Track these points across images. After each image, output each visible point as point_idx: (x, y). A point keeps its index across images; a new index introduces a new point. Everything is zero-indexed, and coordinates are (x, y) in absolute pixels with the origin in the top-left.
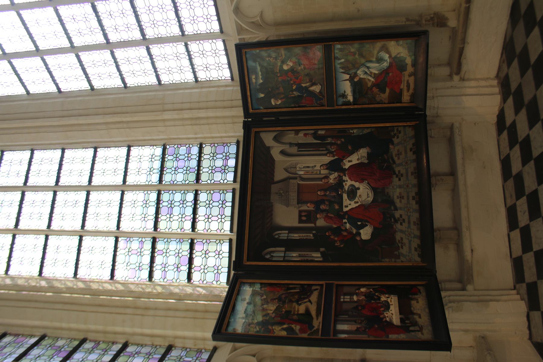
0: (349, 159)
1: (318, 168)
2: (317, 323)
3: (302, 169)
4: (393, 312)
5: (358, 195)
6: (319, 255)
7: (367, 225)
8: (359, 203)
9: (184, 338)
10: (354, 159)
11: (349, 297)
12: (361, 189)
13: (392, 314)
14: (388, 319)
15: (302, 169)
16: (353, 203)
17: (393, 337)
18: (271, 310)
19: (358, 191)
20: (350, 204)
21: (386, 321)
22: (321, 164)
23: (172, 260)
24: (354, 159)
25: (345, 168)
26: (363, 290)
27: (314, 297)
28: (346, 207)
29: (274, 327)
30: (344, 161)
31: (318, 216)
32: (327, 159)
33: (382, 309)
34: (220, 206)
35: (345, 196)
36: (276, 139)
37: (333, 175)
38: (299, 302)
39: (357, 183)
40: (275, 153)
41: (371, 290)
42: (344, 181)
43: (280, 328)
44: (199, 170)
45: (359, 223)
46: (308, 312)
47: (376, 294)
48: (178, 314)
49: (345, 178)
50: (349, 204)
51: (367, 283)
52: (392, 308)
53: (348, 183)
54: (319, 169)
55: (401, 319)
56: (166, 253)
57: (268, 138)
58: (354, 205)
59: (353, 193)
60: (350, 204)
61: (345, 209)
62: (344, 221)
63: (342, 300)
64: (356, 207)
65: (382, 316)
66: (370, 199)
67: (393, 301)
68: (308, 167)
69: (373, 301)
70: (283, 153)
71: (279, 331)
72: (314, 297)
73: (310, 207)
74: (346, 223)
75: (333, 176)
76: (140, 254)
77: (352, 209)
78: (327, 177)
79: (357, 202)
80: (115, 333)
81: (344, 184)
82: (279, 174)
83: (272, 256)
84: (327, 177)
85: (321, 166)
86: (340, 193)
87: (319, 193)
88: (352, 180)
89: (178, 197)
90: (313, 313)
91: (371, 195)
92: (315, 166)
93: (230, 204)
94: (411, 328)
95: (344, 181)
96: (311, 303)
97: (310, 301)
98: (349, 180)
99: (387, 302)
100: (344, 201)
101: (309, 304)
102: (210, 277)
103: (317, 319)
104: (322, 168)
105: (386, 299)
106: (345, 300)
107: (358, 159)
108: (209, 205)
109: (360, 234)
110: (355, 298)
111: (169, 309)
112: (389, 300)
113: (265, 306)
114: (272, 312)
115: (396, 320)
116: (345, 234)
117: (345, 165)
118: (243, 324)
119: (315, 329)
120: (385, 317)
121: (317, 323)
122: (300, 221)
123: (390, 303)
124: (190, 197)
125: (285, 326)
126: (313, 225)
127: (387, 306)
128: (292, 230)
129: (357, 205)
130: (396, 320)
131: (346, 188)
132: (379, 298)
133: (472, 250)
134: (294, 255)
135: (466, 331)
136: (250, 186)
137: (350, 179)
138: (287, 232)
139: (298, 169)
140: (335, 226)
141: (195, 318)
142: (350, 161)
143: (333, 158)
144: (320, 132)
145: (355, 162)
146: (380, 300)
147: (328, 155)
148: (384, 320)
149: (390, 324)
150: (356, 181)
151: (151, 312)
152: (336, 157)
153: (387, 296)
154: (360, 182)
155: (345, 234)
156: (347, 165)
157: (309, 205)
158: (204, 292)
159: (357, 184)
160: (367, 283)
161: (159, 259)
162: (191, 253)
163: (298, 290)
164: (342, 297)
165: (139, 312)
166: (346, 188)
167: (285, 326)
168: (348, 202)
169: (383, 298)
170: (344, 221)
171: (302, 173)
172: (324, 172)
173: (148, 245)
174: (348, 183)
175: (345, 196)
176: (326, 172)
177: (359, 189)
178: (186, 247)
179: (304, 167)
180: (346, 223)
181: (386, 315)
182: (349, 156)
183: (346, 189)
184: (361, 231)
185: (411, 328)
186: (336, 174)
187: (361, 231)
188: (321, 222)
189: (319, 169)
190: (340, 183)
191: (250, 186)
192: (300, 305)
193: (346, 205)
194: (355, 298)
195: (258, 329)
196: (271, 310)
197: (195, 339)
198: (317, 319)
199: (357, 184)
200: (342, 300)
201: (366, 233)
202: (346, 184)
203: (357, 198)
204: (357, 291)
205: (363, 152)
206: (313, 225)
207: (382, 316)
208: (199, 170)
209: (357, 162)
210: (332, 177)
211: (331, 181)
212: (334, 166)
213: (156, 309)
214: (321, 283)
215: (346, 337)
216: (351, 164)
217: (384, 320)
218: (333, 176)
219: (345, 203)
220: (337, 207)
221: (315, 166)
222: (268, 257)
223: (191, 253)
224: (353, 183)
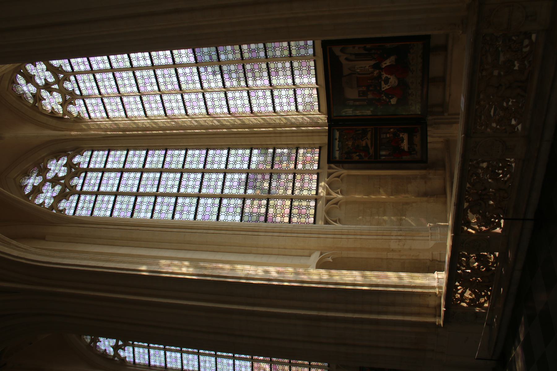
0: (385, 62)
1: (367, 67)
2: (371, 151)
3: (359, 69)
4: (405, 144)
5: (390, 82)
6: (370, 112)
7: (394, 97)
8: (390, 86)
9: (304, 144)
10: (387, 63)
11: (385, 135)
12: (391, 79)
13: (405, 145)
14: (402, 148)
15: (359, 69)
16: (387, 86)
17: (405, 158)
18: (350, 145)
19: (390, 80)
20: (385, 87)
21: (402, 149)
22: (369, 65)
23: (285, 100)
24: (387, 63)
25: (383, 68)
26: (392, 130)
27: (369, 136)
28: (383, 88)
29: (353, 155)
30: (382, 63)
31: (369, 93)
32: (372, 63)
33: (400, 142)
34: (307, 69)
35: (383, 83)
36: (342, 51)
37: (376, 72)
38: (363, 139)
39: (389, 76)
40: (342, 59)
41: (396, 130)
42: (382, 75)
43: (356, 155)
44: (290, 48)
45: (390, 96)
46: (367, 144)
47: (398, 133)
48: (299, 134)
49: (382, 73)
50: (385, 87)
51: (393, 127)
52: (405, 141)
53: (384, 76)
54: (368, 68)
55: (408, 147)
56: (280, 97)
57: (337, 50)
58: (387, 87)
59: (387, 81)
60: (385, 87)
61: (383, 90)
62: (382, 95)
63: (382, 137)
64: (388, 88)
65: (400, 146)
66: (397, 84)
67: (405, 136)
68: (362, 67)
69: (396, 137)
70: (347, 59)
71: (356, 157)
72: (369, 136)
73: (364, 89)
74: (383, 96)
75: (376, 73)
76: (265, 98)
77: (387, 89)
78: (372, 73)
79: (389, 86)
80: (267, 145)
81: (382, 76)
82: (346, 72)
83: (346, 113)
84: (372, 73)
85: (369, 67)
86: (380, 81)
87: (368, 81)
88: (386, 74)
89: (280, 65)
90: (369, 145)
91: (397, 82)
92: (366, 67)
93: (314, 68)
94: (413, 153)
95: (382, 75)
96: (368, 139)
97: (367, 138)
98: (385, 74)
99: (402, 137)
100: (382, 85)
101: (367, 140)
102: (308, 107)
103: (371, 149)
104: (370, 67)
105: (402, 136)
106: (384, 137)
107: (390, 62)
108: (300, 69)
109: (390, 101)
110: (388, 136)
111: (293, 133)
112: (404, 136)
113: (347, 143)
114: (350, 146)
115: (406, 148)
116: (383, 101)
117: (382, 66)
118: (339, 154)
119: (371, 154)
120: (401, 147)
121: (371, 151)
122: (359, 96)
123: (404, 138)
124: (288, 65)
125: (358, 154)
126: (366, 98)
127: (402, 140)
128: (355, 100)
129: (389, 87)
130: (406, 148)
131: (383, 78)
132: (399, 135)
133: (450, 95)
134: (357, 112)
135: (440, 137)
136: (330, 80)
137: (385, 73)
138: (353, 101)
139: (356, 68)
140: (377, 98)
141: (308, 136)
142: (386, 64)
143: (375, 62)
144: (367, 47)
145: (388, 64)
146: (399, 136)
147: (373, 60)
148: (401, 148)
149: (403, 150)
150: (389, 75)
151: (284, 135)
152: (377, 61)
153: (403, 134)
154: (390, 75)
155: (383, 101)
156: (384, 66)
157: (363, 88)
158: (309, 120)
159: (389, 76)
160: (393, 127)
161: (277, 101)
162: (295, 96)
163: (361, 132)
164: (382, 135)
165: (278, 135)
166: (383, 78)
167: (358, 154)
168: (385, 86)
169: (401, 136)
170: (382, 95)
171: (358, 71)
172: (370, 70)
173: (268, 93)
174: (384, 76)
175: (383, 83)
176: (372, 70)
177: (390, 79)
178: (291, 92)
179: (359, 68)
180: (383, 96)
181: (402, 145)
182: (384, 61)
183: (383, 79)
184: (391, 100)
185: (413, 153)
186: (378, 71)
187: (391, 100)
188: (370, 96)
189: (368, 68)
190: (380, 76)
191: (330, 80)
192: (363, 141)
193: (383, 87)
194: (388, 136)
195: (346, 156)
196: (350, 145)
197: (309, 144)
198: (371, 149)
199: (389, 76)
200: (382, 137)
201: (393, 101)
202: (383, 76)
203: (389, 84)
204: (389, 131)
205: (393, 58)
206: (366, 98)
207: (400, 146)
208: (290, 48)
209: (389, 64)
210: (375, 73)
211: (375, 75)
212: (376, 66)
213: (286, 133)
214: (372, 127)
215: (384, 159)
216: (386, 65)
217: (401, 148)
218: (376, 73)
219: (382, 87)
220: (378, 88)
221: (366, 67)
222: (344, 114)
223: (295, 96)
224: (387, 75)
